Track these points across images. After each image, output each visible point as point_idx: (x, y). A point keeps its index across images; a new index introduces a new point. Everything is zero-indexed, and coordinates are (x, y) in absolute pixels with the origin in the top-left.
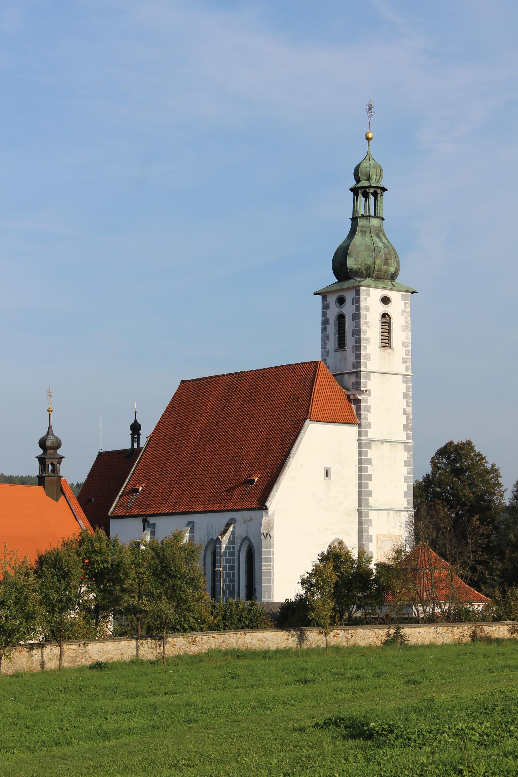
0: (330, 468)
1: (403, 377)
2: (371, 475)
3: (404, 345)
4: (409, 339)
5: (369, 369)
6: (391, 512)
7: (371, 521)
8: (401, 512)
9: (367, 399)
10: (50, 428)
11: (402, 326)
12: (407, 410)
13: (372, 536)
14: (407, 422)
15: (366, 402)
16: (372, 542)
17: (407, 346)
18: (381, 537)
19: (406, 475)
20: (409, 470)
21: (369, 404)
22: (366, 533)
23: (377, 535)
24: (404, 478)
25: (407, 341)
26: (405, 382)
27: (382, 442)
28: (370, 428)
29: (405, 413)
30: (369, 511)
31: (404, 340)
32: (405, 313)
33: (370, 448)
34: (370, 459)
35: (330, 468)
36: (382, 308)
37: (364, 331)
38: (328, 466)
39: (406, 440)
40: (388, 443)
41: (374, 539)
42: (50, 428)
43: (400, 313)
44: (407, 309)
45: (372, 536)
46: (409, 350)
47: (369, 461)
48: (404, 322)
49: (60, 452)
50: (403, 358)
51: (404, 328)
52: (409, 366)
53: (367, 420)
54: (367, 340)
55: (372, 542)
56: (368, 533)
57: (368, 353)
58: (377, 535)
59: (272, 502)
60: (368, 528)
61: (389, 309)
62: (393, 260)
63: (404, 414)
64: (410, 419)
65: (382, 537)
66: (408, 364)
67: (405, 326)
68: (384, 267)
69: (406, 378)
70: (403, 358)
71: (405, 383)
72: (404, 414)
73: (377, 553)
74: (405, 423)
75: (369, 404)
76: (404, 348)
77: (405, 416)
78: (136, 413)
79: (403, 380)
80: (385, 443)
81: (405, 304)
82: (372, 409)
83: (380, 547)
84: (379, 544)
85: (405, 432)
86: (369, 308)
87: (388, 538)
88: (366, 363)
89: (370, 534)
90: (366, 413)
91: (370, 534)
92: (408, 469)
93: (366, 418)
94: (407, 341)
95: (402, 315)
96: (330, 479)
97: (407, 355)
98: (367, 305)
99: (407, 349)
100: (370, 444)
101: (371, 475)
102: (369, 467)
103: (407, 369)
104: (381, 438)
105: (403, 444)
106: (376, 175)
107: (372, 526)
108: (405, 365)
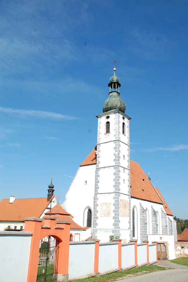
2: (99, 181)
14: (115, 158)
15: (99, 155)
18: (102, 204)
26: (115, 143)
27: (104, 168)
29: (115, 154)
41: (99, 205)
44: (116, 117)
47: (99, 176)
56: (97, 203)
61: (109, 120)
77: (115, 156)
81: (116, 116)
82: (101, 157)
83: (101, 208)
85: (115, 162)
93: (98, 160)
97: (116, 133)
100: (99, 169)
101: (99, 181)
102: (99, 178)
108: (115, 137)
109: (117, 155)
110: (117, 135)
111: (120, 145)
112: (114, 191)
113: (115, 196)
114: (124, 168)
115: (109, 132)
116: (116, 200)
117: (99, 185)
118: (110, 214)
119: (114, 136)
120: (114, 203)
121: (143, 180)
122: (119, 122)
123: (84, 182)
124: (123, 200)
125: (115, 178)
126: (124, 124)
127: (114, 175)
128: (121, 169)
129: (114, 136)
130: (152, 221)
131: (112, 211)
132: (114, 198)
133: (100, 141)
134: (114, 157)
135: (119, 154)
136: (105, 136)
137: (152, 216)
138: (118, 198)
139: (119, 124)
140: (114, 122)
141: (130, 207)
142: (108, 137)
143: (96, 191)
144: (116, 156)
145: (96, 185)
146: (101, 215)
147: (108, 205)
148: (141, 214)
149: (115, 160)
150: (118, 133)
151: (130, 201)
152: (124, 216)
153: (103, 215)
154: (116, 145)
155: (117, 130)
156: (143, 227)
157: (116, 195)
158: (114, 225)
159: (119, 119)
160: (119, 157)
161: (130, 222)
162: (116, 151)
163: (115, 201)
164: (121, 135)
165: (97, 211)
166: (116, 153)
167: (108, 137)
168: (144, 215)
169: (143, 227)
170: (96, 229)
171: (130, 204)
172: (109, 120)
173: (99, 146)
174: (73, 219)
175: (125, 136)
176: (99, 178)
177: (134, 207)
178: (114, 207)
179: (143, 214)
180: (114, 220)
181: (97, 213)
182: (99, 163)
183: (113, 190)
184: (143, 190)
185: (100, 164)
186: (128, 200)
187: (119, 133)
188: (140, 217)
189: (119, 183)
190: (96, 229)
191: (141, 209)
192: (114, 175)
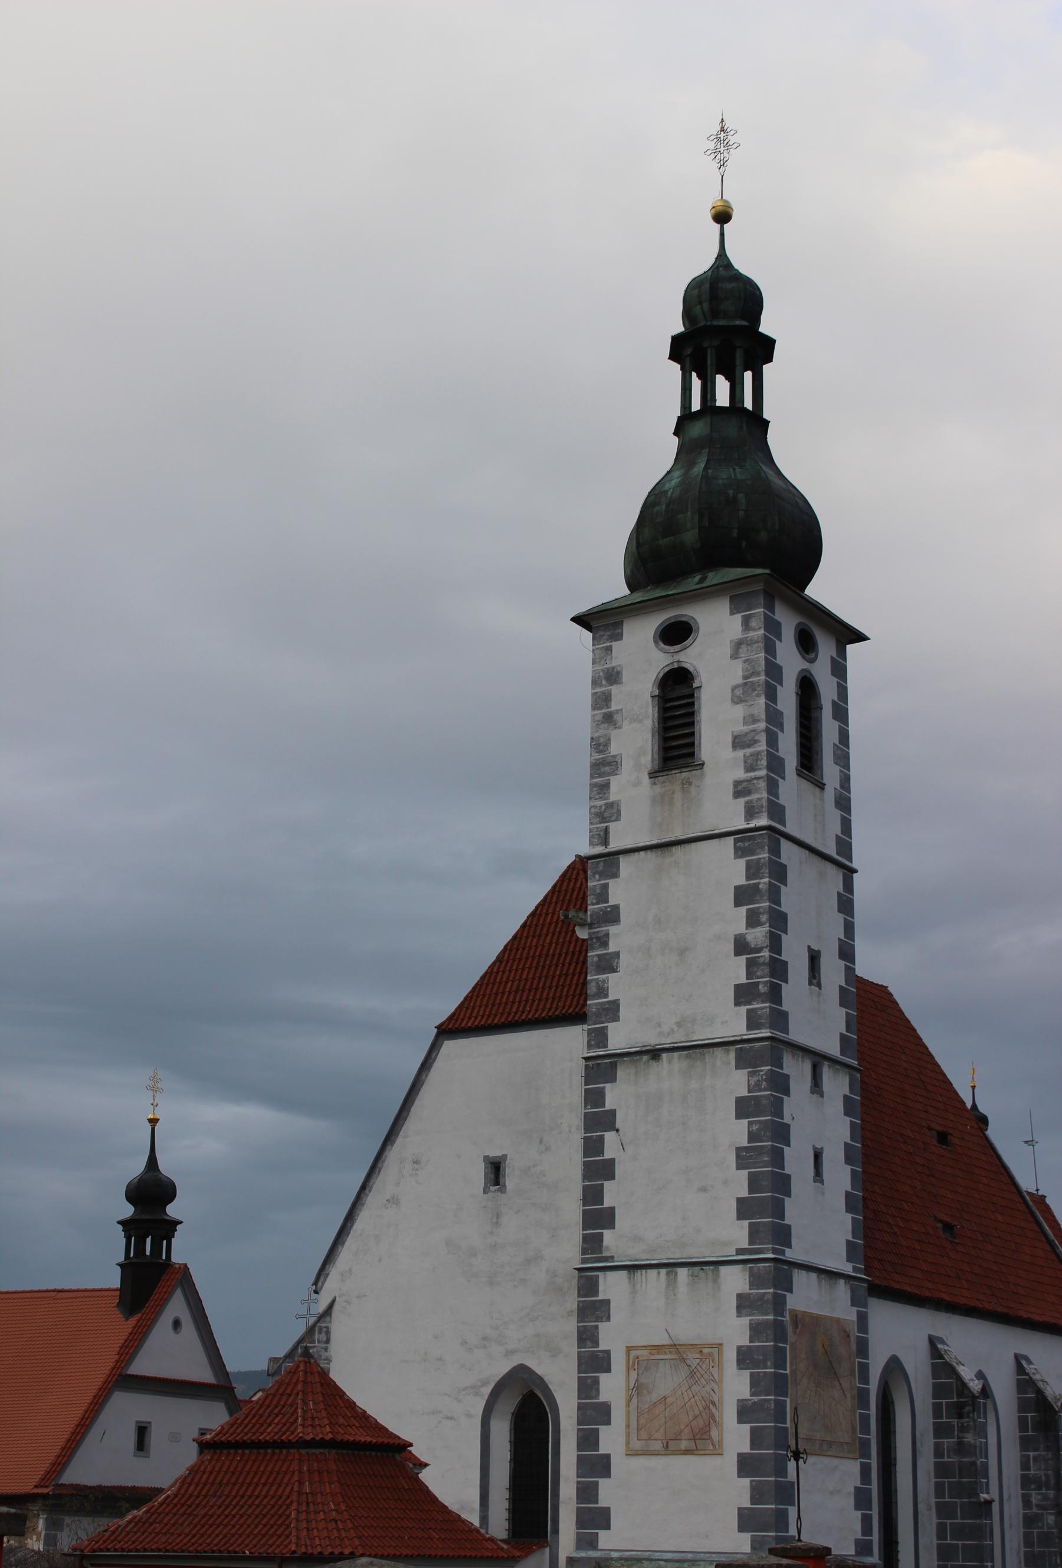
0: (504, 1157)
1: (736, 841)
2: (612, 1162)
3: (739, 742)
4: (759, 721)
5: (614, 845)
6: (683, 1273)
7: (607, 1303)
8: (723, 1269)
9: (607, 935)
10: (152, 1161)
11: (734, 689)
12: (749, 938)
13: (608, 1353)
14: (749, 975)
16: (608, 1370)
17: (754, 742)
18: (644, 1353)
19: (745, 1144)
20: (755, 1127)
21: (612, 948)
22: (589, 1343)
23: (629, 1349)
24: (738, 1156)
25: (751, 727)
26: (739, 853)
27: (655, 1053)
28: (616, 1018)
29: (741, 946)
30: (601, 1274)
31: (741, 728)
32: (744, 648)
33: (613, 1079)
34: (613, 1113)
35: (504, 1157)
36: (660, 660)
37: (602, 740)
38: (495, 1153)
39: (744, 1031)
40: (676, 1054)
41: (618, 1362)
42: (152, 1161)
43: (728, 650)
44: (751, 634)
45: (608, 1353)
46: (759, 753)
48: (740, 673)
49: (173, 1210)
50: (737, 783)
51: (739, 692)
52: (759, 799)
53: (607, 996)
54: (609, 764)
55: (608, 1370)
57: (613, 798)
58: (629, 1349)
59: (328, 1275)
60: (597, 1327)
61: (692, 656)
62: (689, 513)
63: (738, 952)
64: (764, 964)
65: (645, 1352)
66: (754, 797)
67: (745, 684)
68: (664, 542)
69: (750, 838)
70: (737, 783)
71: (741, 857)
72: (738, 952)
73: (628, 1405)
74: (743, 980)
75: (612, 948)
76: (740, 754)
77: (742, 960)
78: (973, 1087)
79: (736, 849)
80: (664, 1056)
82: (624, 962)
84: (634, 1375)
85: (743, 1009)
86: (618, 673)
87: (668, 1356)
88: (606, 831)
89: (602, 1347)
90: (602, 977)
91: (602, 1347)
92: (750, 1123)
93: (603, 991)
94: (751, 727)
95: (734, 656)
96: (503, 1190)
97: (749, 768)
98: (614, 664)
99: (748, 751)
100: (614, 1066)
101: (612, 1162)
102: (609, 1137)
103: (751, 812)
104: (651, 1039)
105: (732, 1048)
106: (700, 303)
107: (608, 1319)
108: (742, 801)
109: (766, 954)
110: (762, 784)
111: (779, 873)
112: (745, 1244)
113: (752, 1285)
114: (818, 1059)
115: (692, 755)
116: (751, 1318)
117: (612, 1195)
118: (714, 1433)
119: (737, 794)
120: (745, 1341)
121: (943, 1138)
122: (774, 671)
123: (479, 1173)
124: (816, 1320)
125: (752, 1137)
126: (807, 687)
127: (739, 1115)
128: (797, 1071)
129: (737, 794)
130: (1026, 1482)
131: (729, 1413)
132: (744, 1304)
133: (613, 826)
134: (737, 971)
135: (775, 943)
136: (658, 789)
137: (1025, 1443)
138: (779, 1304)
139: (771, 695)
140: (736, 672)
141: (864, 1370)
142: (678, 796)
143: (592, 1244)
144: (751, 965)
145: (592, 1195)
146: (637, 1445)
147: (693, 1358)
148: (940, 1431)
149: (743, 994)
150: (769, 768)
151: (863, 1320)
152: (827, 1447)
153: (657, 1446)
154: (752, 871)
155: (762, 746)
156: (959, 1532)
157: (755, 1280)
158: (746, 1521)
159: (770, 649)
160: (779, 969)
161: (861, 1499)
162: (752, 920)
163: (756, 1330)
164: (791, 786)
165: (603, 1413)
166: (758, 935)
167: (678, 796)
168: (969, 1438)
169: (959, 1532)
170: (592, 1554)
171: (863, 1348)
172: (692, 656)
173: (604, 875)
174: (425, 1476)
175: (821, 786)
176: (609, 1137)
177: (894, 1366)
178: (746, 1374)
179: (963, 1429)
180: (746, 1482)
181: (603, 1429)
182: (612, 1011)
183: (738, 1234)
184: (948, 1227)
185: (616, 1018)
186: (849, 1315)
187: (776, 765)
188: (938, 1452)
189: (783, 1184)
190: (592, 1554)
191: (938, 1391)
192: (739, 1115)
